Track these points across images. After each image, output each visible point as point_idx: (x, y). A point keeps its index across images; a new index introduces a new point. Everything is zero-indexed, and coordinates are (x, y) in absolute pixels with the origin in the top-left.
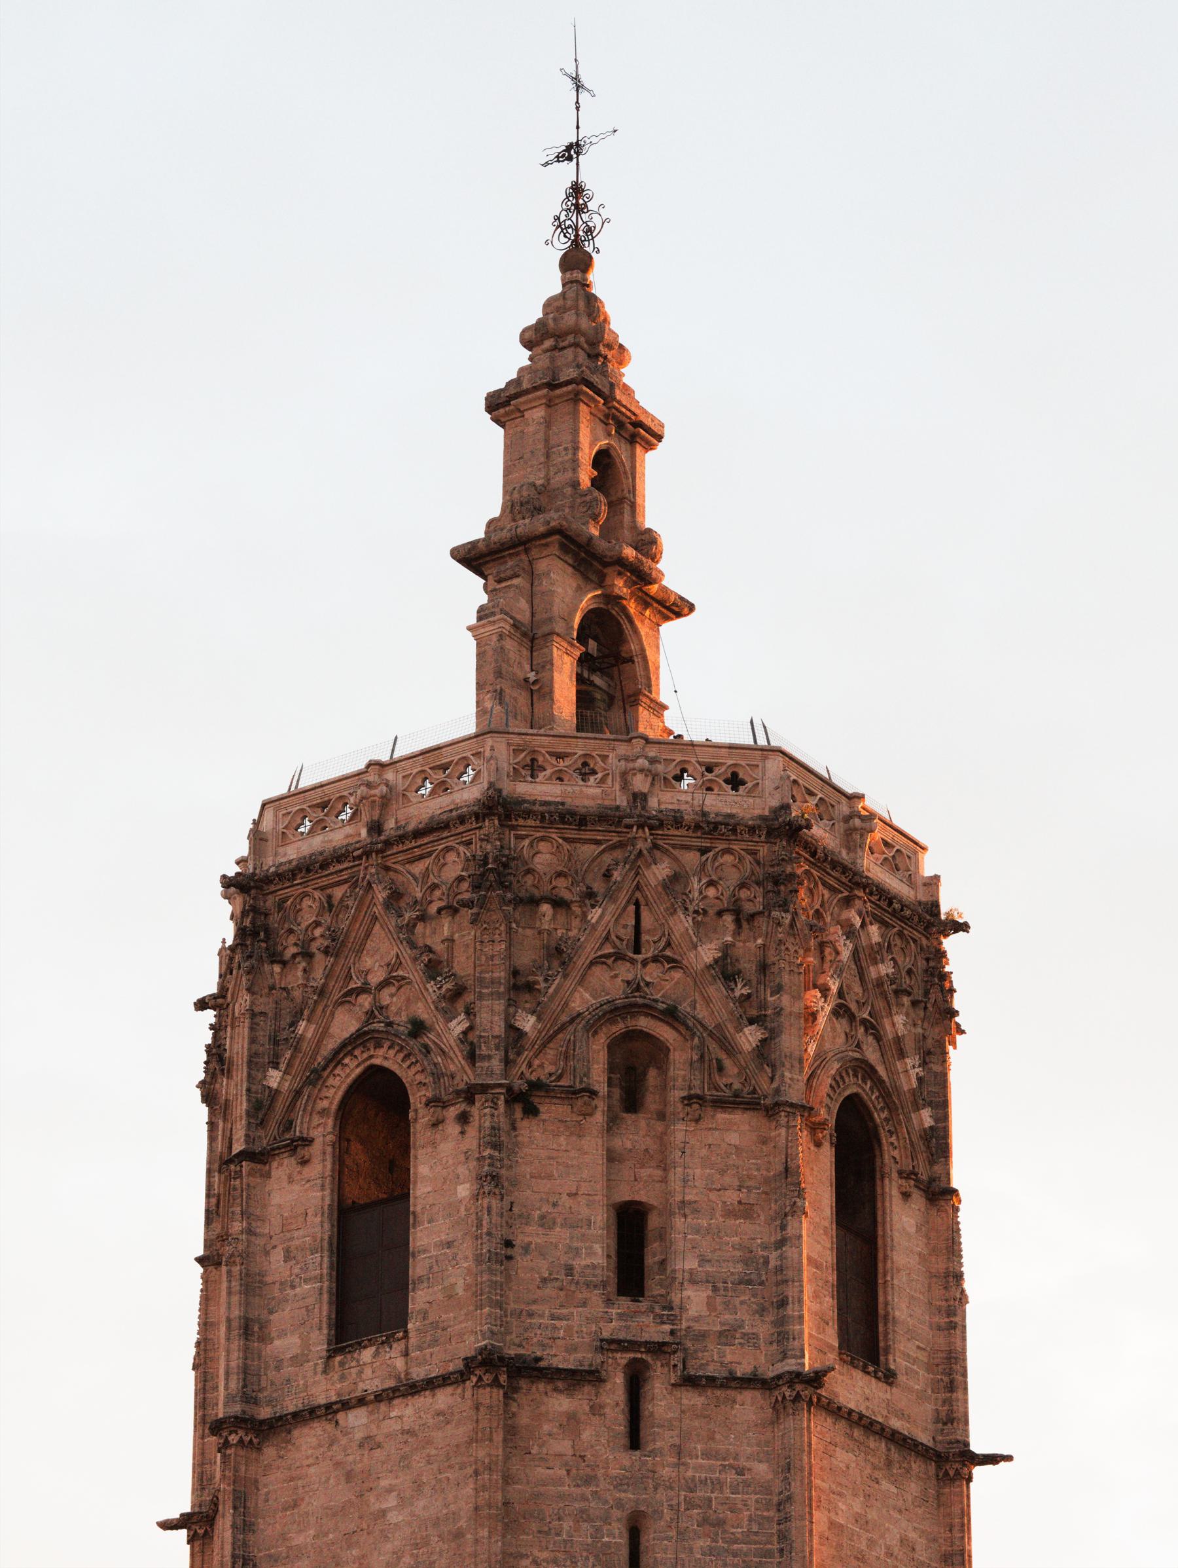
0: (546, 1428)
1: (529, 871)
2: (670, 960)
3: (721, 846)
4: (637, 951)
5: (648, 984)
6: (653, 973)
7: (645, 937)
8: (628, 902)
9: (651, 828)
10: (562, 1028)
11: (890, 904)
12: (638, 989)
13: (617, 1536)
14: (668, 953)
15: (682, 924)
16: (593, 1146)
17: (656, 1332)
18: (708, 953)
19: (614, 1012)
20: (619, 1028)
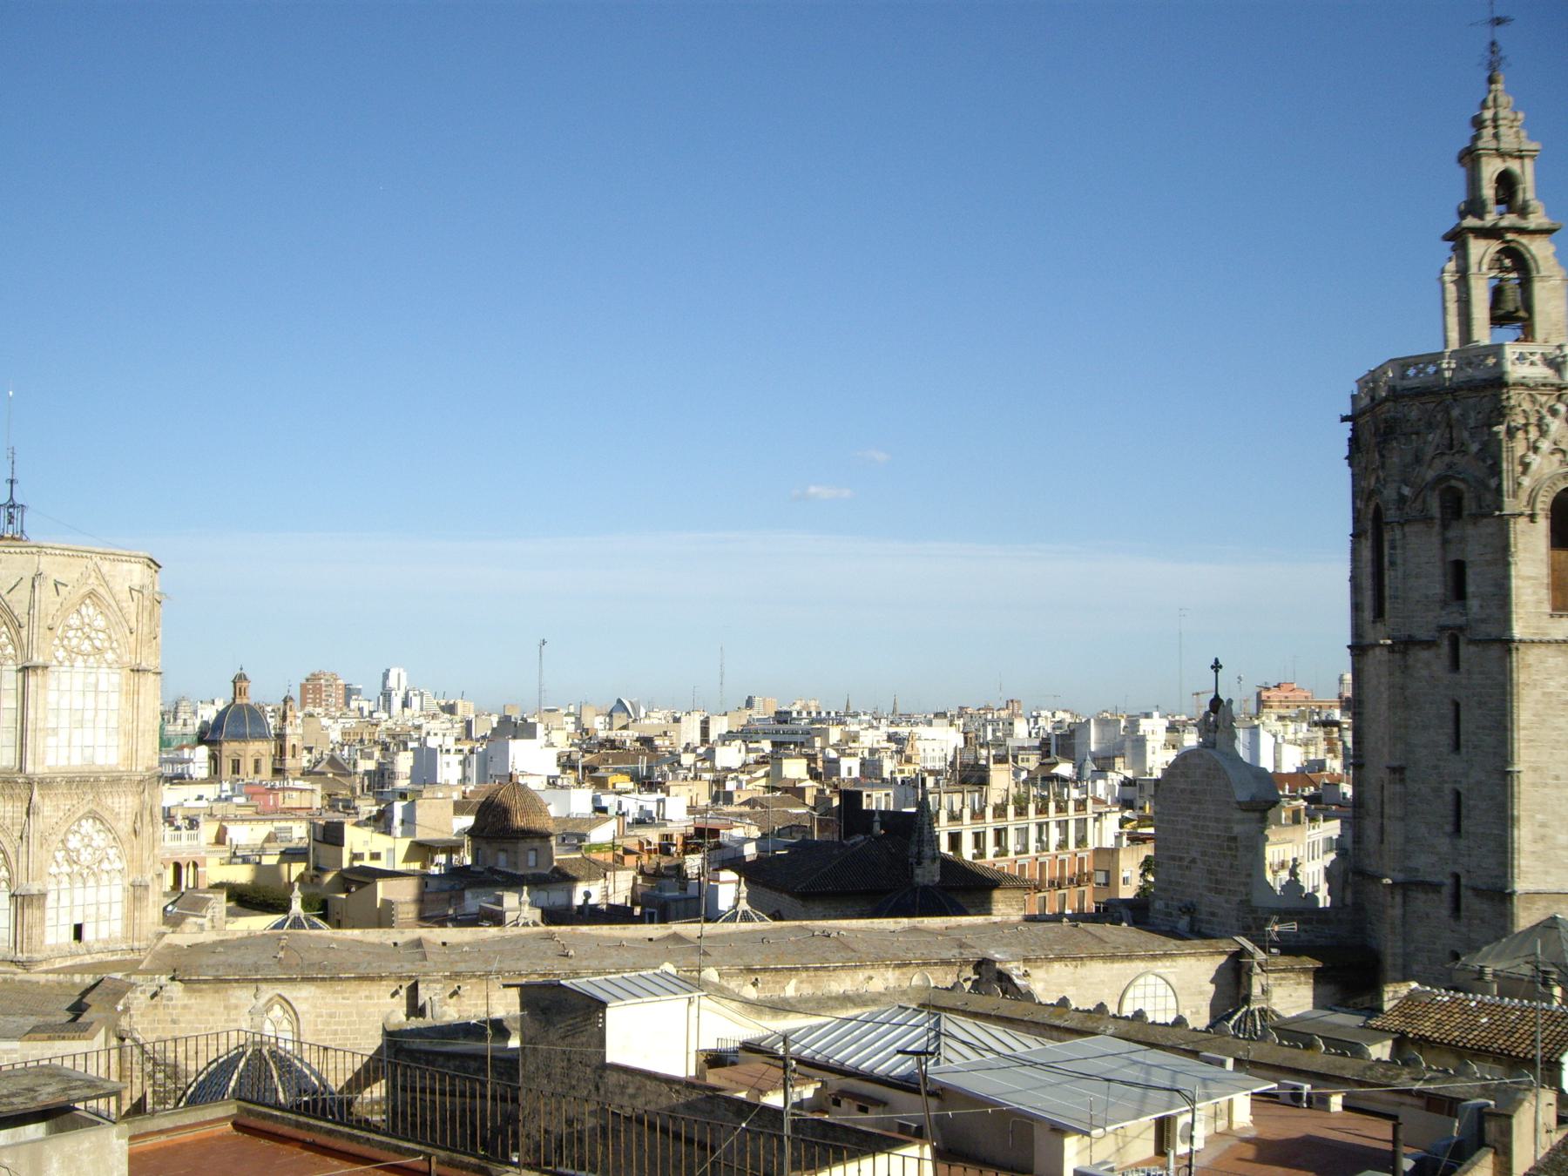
13: (1448, 710)
15: (1466, 434)
16: (1436, 540)
17: (1461, 620)
18: (1474, 448)
19: (1440, 479)
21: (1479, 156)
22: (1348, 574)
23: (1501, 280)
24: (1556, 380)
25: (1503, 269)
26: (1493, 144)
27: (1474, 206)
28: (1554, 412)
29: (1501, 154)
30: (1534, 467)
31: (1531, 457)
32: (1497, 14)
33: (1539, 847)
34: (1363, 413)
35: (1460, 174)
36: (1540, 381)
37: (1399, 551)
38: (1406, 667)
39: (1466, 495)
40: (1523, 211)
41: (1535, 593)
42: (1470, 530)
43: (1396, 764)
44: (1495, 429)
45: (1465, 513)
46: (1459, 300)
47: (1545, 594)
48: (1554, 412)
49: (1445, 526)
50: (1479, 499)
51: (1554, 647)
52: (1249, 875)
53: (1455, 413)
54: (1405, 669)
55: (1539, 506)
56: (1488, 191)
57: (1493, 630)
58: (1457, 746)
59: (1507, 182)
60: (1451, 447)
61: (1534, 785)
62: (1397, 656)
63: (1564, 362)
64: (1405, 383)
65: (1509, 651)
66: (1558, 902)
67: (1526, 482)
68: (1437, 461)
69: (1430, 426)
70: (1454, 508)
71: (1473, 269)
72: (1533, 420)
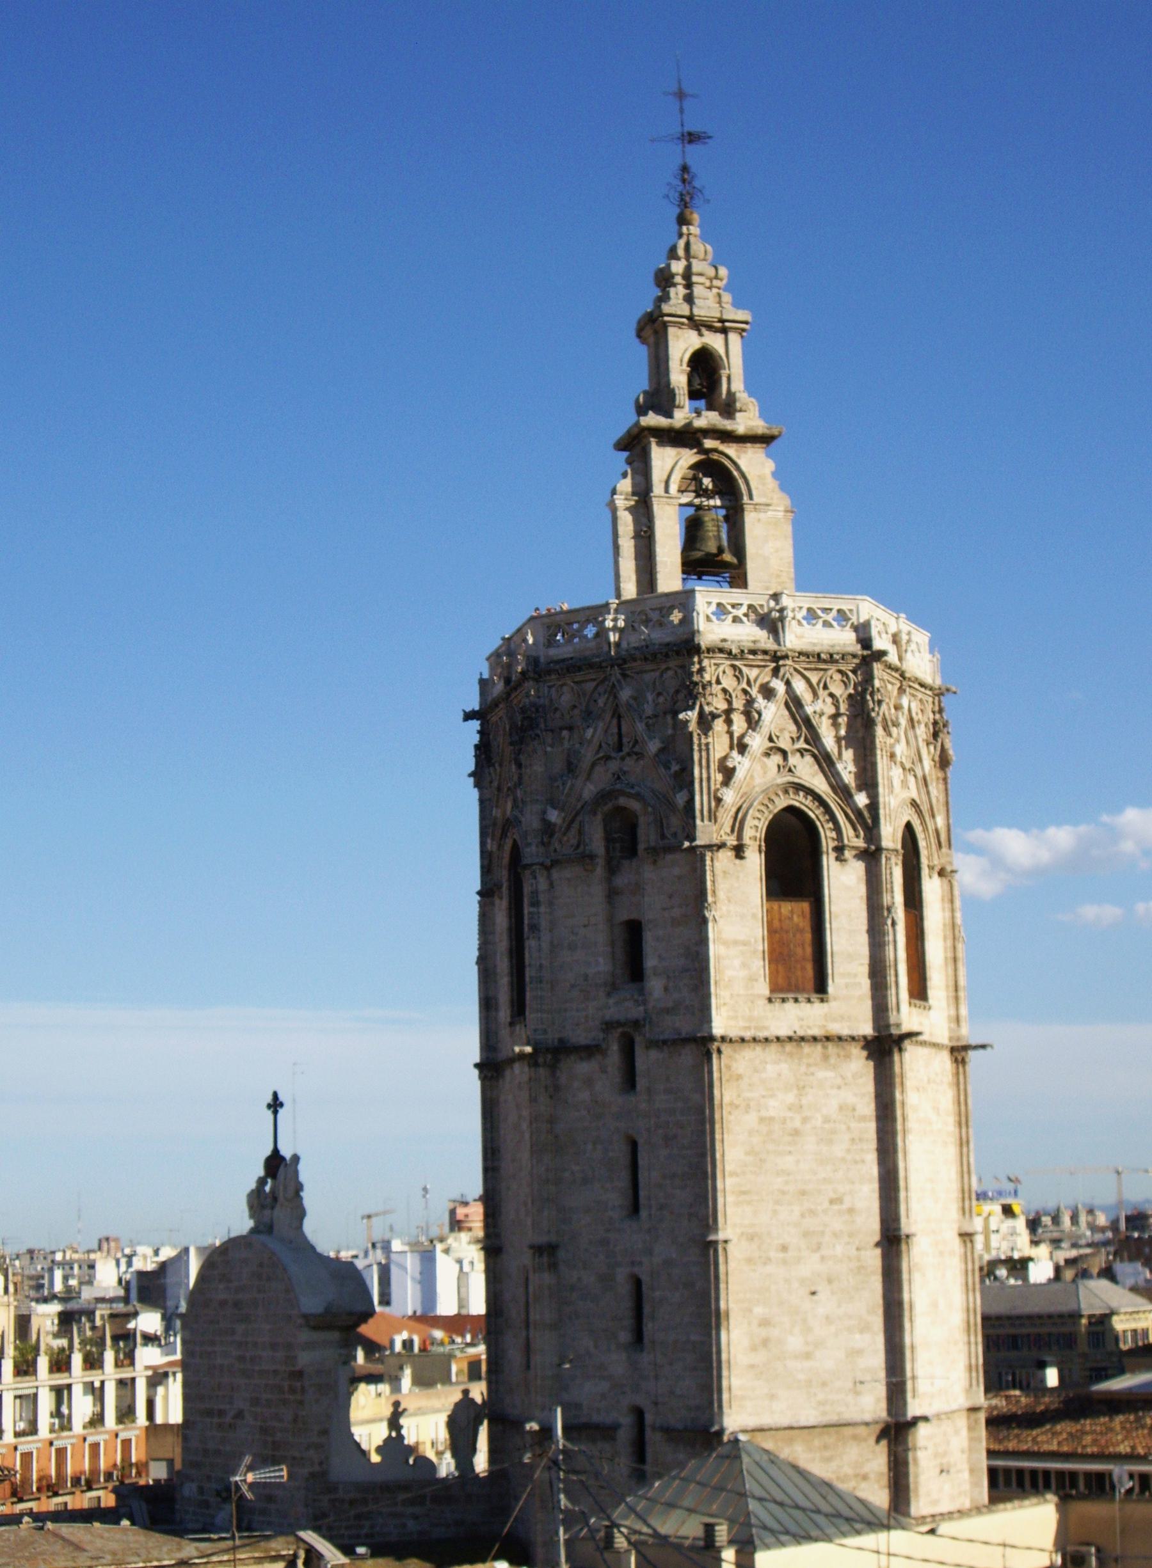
0: (576, 1084)
1: (556, 709)
2: (636, 754)
3: (663, 667)
4: (620, 749)
5: (625, 773)
6: (629, 763)
7: (625, 740)
8: (613, 717)
9: (619, 666)
10: (577, 814)
11: (819, 655)
12: (619, 778)
13: (620, 1152)
14: (636, 749)
15: (640, 727)
16: (598, 891)
17: (636, 1012)
18: (653, 746)
19: (604, 796)
20: (610, 806)
21: (665, 326)
22: (475, 954)
23: (699, 508)
24: (770, 645)
25: (701, 492)
26: (685, 310)
27: (659, 398)
28: (768, 693)
29: (696, 324)
30: (739, 775)
31: (736, 758)
32: (690, 127)
33: (760, 1358)
34: (495, 704)
35: (641, 354)
36: (748, 645)
37: (542, 909)
38: (557, 1088)
39: (642, 820)
40: (729, 409)
41: (744, 965)
42: (649, 873)
43: (543, 1239)
44: (681, 716)
45: (641, 847)
46: (637, 536)
47: (759, 967)
48: (768, 693)
49: (612, 869)
50: (660, 825)
51: (774, 1047)
52: (325, 1432)
53: (625, 694)
54: (555, 1090)
55: (748, 833)
56: (679, 378)
57: (683, 1024)
58: (635, 1208)
59: (704, 365)
60: (620, 748)
61: (749, 1261)
62: (542, 1071)
63: (782, 619)
64: (553, 652)
65: (708, 1055)
66: (791, 1441)
67: (730, 796)
68: (599, 769)
69: (589, 715)
70: (625, 841)
71: (658, 489)
72: (739, 703)
